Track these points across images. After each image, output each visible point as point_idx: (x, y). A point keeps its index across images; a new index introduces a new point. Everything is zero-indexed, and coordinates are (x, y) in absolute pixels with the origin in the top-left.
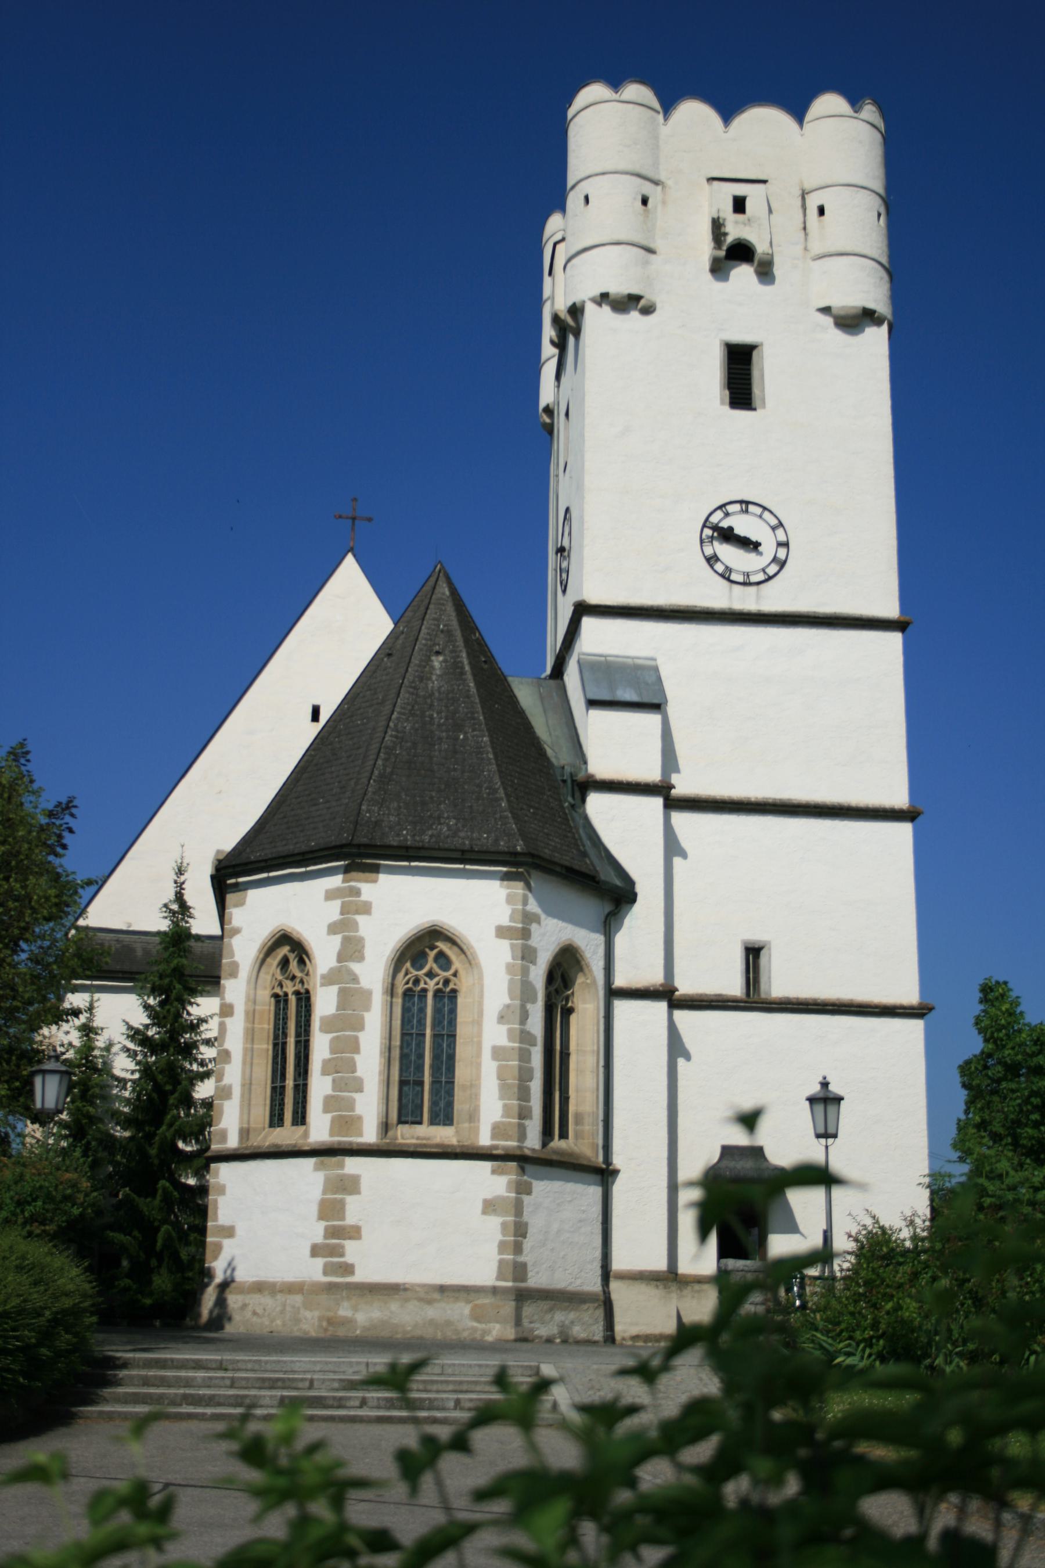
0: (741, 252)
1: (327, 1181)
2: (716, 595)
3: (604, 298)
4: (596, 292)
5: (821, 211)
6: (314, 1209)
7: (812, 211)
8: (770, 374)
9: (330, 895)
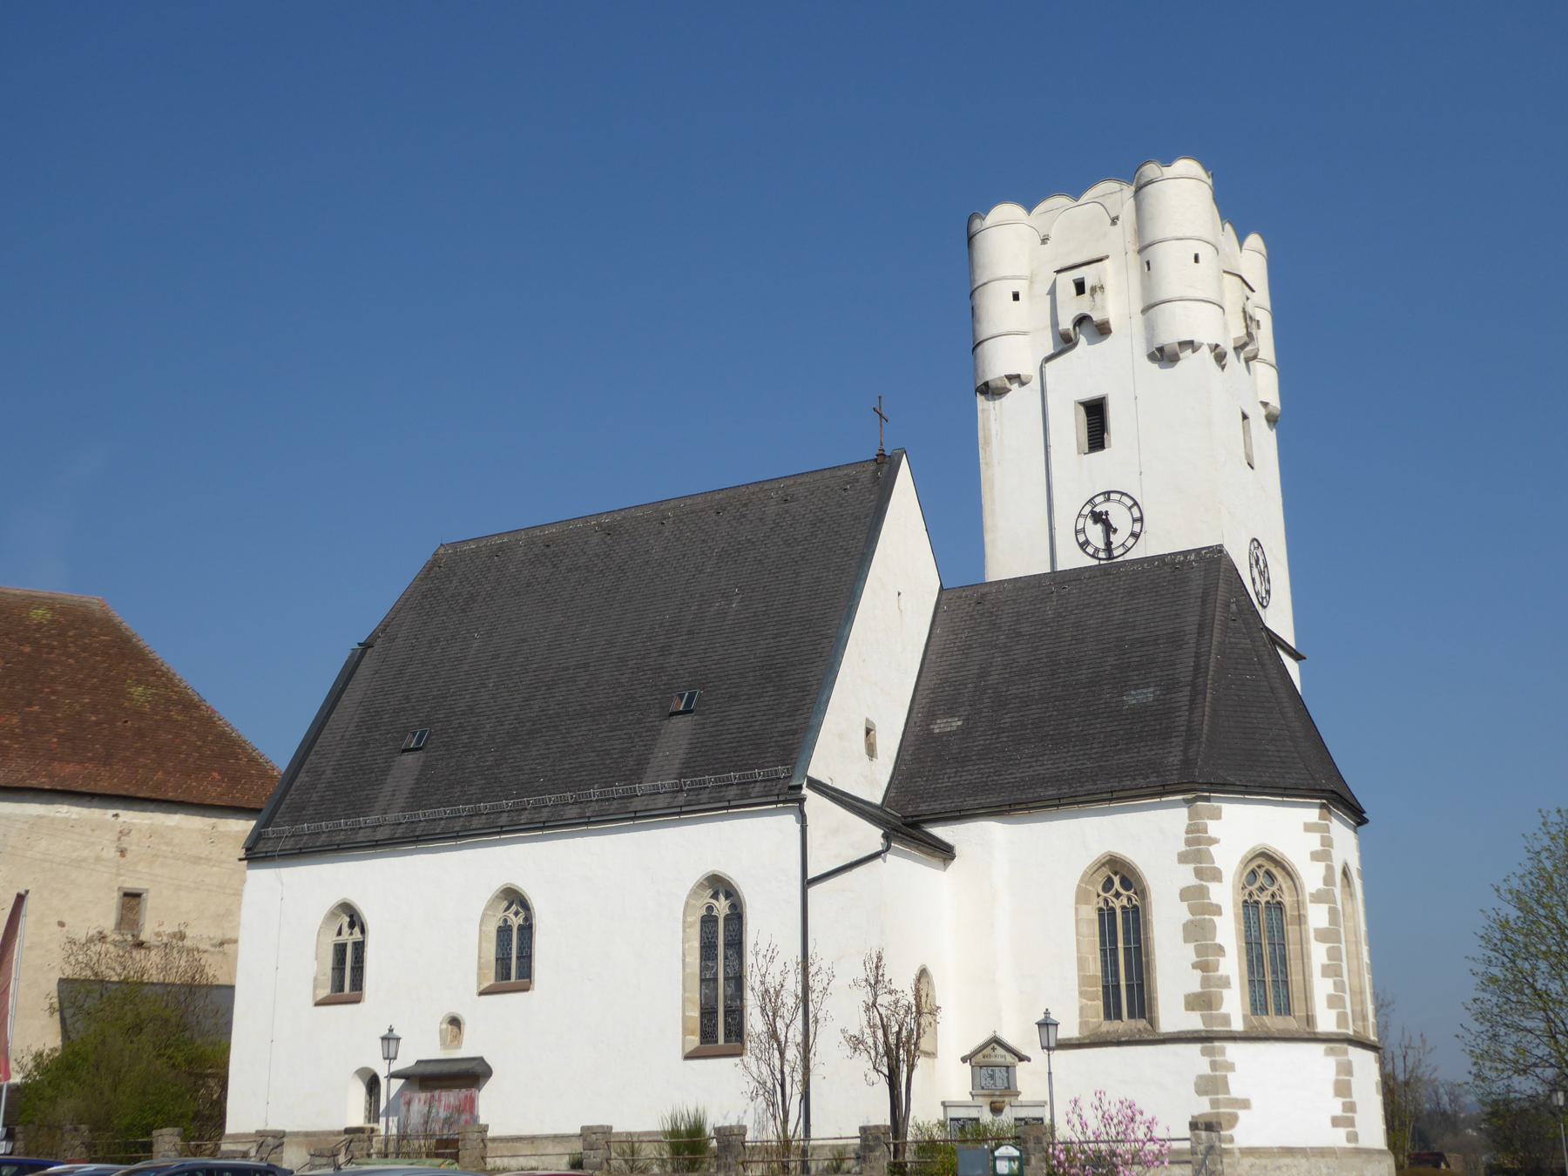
1: (1339, 1064)
4: (1214, 342)
6: (1330, 1090)
9: (1309, 828)
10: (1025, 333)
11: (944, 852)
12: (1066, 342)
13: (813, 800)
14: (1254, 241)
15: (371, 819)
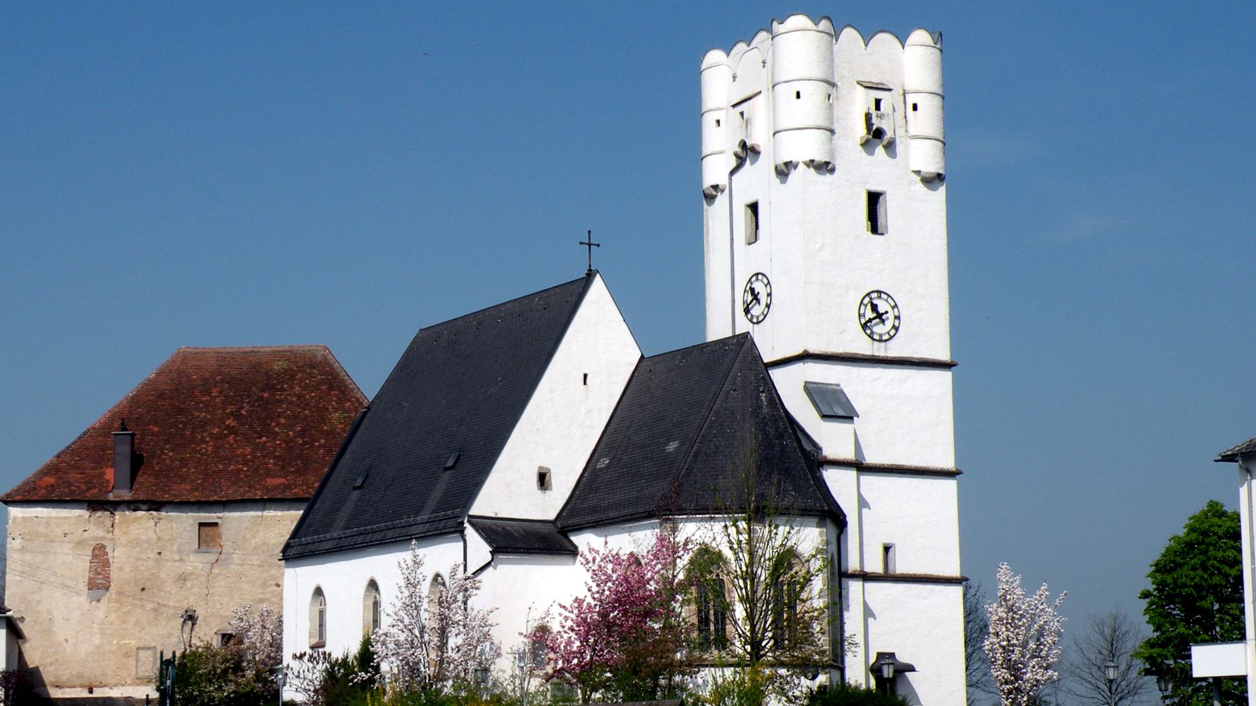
0: (878, 134)
2: (864, 346)
3: (811, 163)
4: (807, 159)
5: (915, 107)
7: (910, 107)
8: (891, 210)
10: (722, 152)
11: (573, 552)
12: (741, 161)
13: (470, 532)
14: (920, 37)
15: (328, 536)
